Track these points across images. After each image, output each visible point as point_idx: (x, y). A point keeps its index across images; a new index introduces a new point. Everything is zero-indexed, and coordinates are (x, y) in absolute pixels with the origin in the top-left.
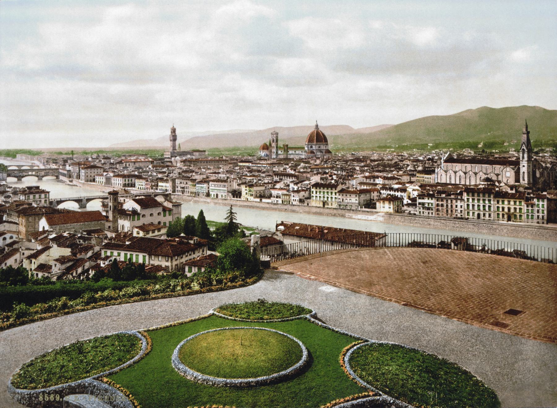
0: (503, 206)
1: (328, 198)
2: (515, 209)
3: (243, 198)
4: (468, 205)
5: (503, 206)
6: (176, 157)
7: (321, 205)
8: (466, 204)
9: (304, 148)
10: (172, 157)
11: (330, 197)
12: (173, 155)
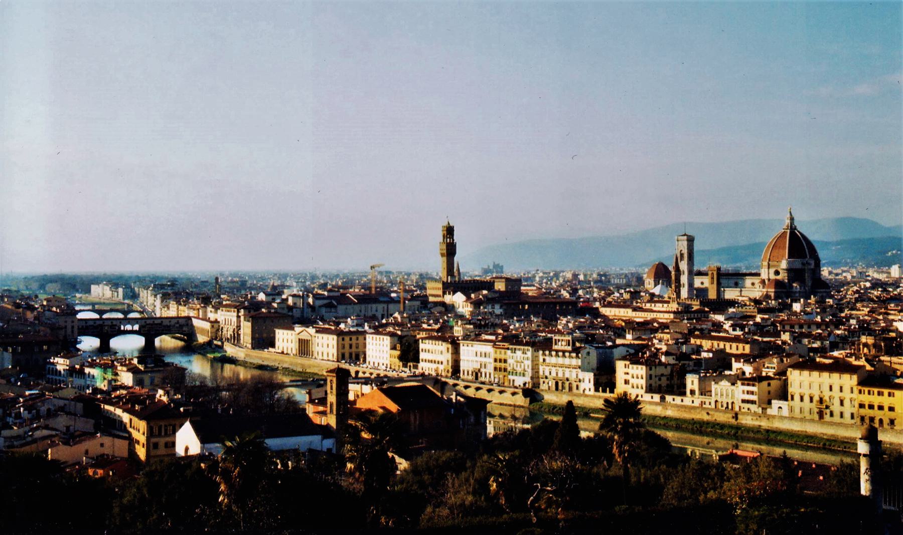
6: (454, 293)
7: (816, 417)
9: (758, 275)
10: (444, 293)
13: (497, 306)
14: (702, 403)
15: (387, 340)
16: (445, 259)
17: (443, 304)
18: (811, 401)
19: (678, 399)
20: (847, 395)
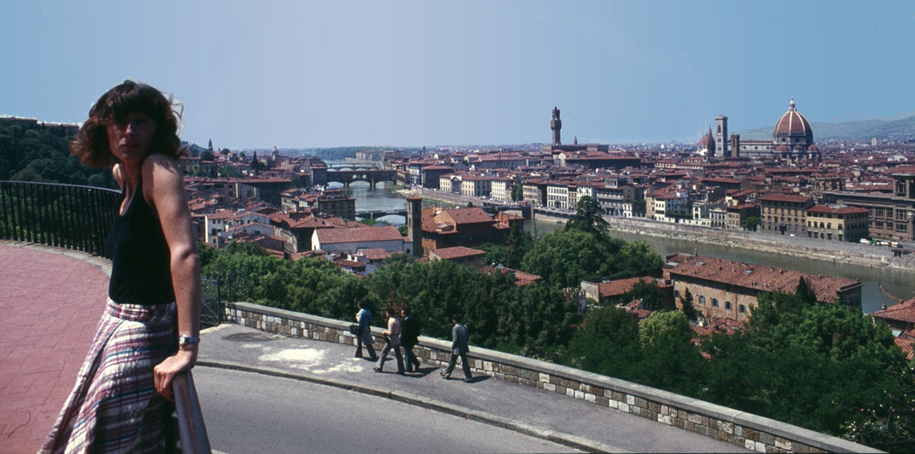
1: (789, 219)
6: (558, 153)
10: (553, 153)
14: (704, 223)
15: (504, 184)
17: (552, 161)
18: (776, 221)
19: (687, 222)
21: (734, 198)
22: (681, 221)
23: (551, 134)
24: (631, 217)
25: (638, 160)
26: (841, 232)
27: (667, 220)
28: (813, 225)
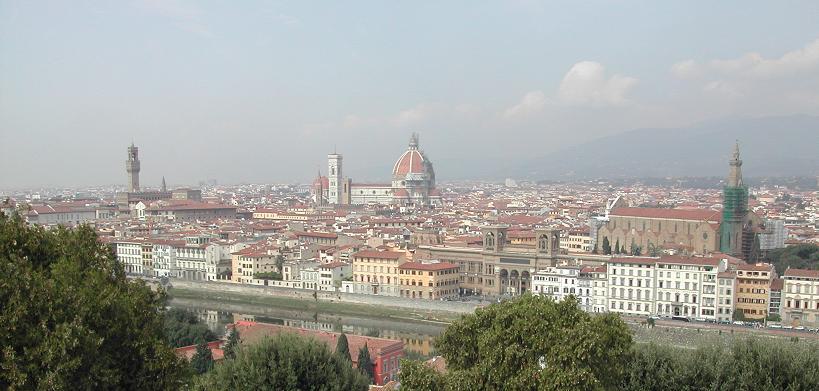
0: (668, 290)
2: (687, 296)
3: (234, 280)
4: (614, 290)
5: (668, 290)
7: (372, 293)
8: (611, 287)
10: (130, 202)
11: (385, 276)
12: (133, 198)
13: (170, 213)
16: (130, 174)
17: (129, 212)
19: (277, 282)
20: (392, 276)
21: (328, 254)
22: (270, 283)
23: (127, 179)
24: (215, 280)
25: (233, 209)
26: (431, 289)
27: (255, 282)
28: (405, 283)
